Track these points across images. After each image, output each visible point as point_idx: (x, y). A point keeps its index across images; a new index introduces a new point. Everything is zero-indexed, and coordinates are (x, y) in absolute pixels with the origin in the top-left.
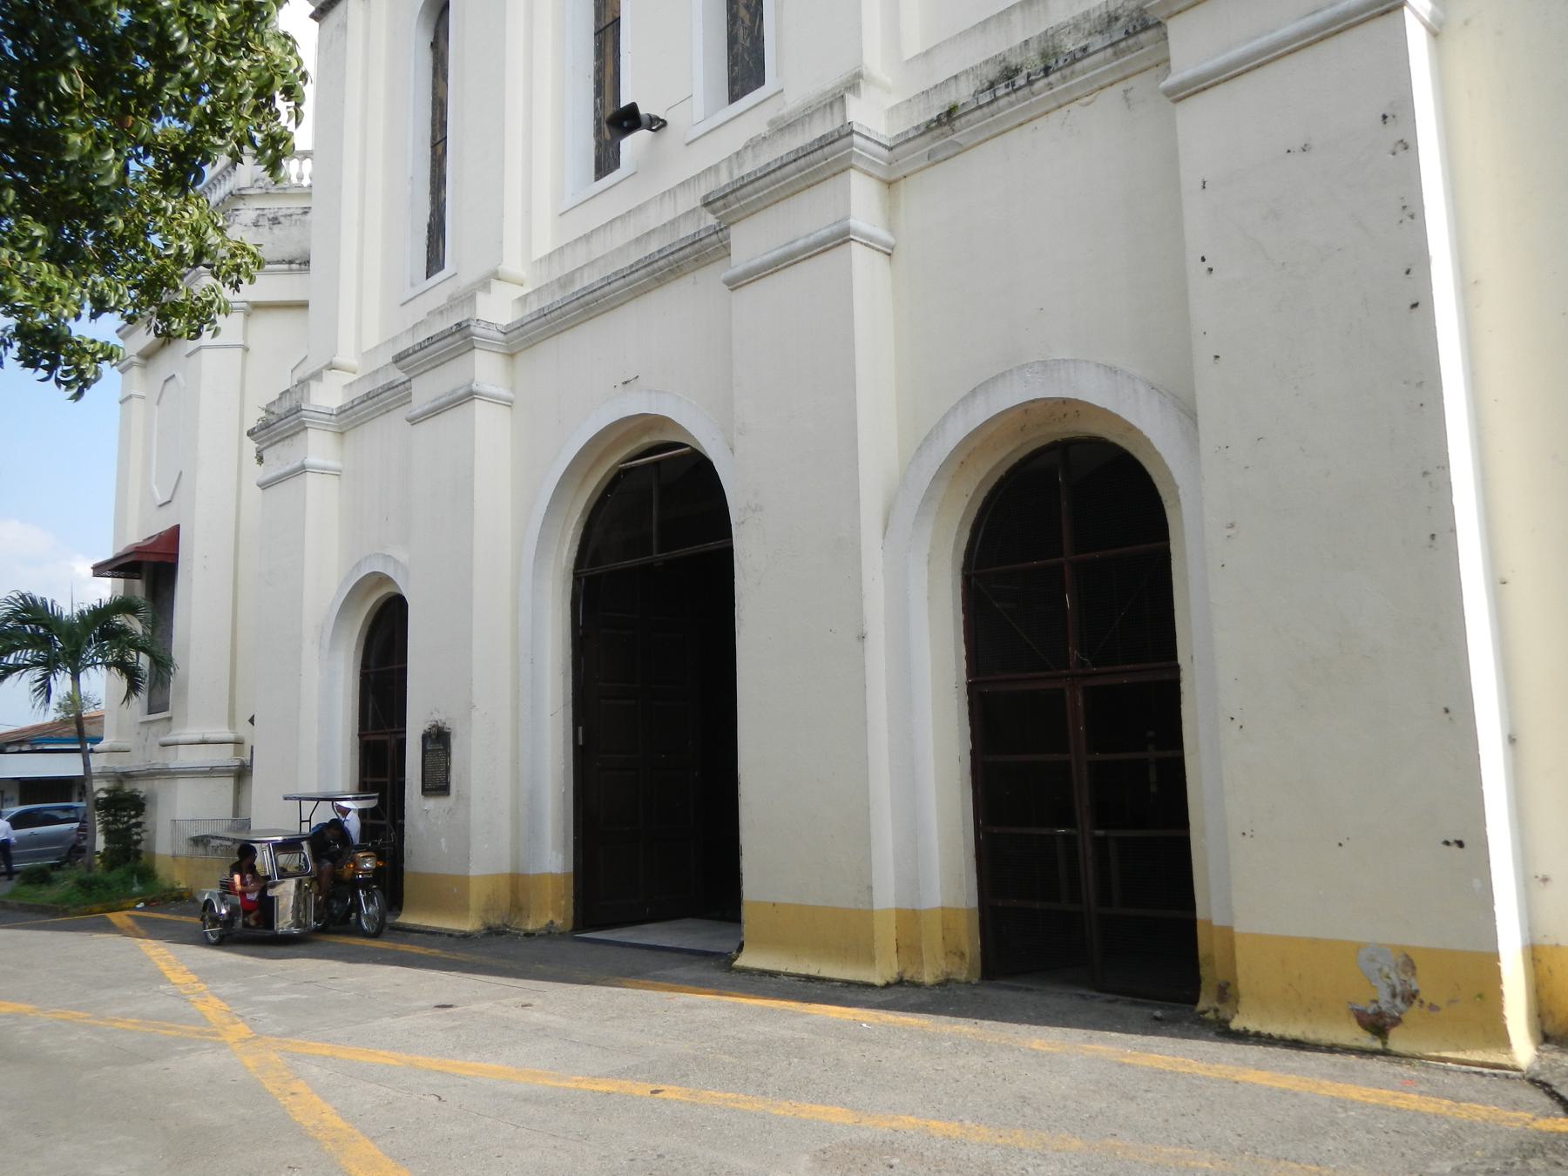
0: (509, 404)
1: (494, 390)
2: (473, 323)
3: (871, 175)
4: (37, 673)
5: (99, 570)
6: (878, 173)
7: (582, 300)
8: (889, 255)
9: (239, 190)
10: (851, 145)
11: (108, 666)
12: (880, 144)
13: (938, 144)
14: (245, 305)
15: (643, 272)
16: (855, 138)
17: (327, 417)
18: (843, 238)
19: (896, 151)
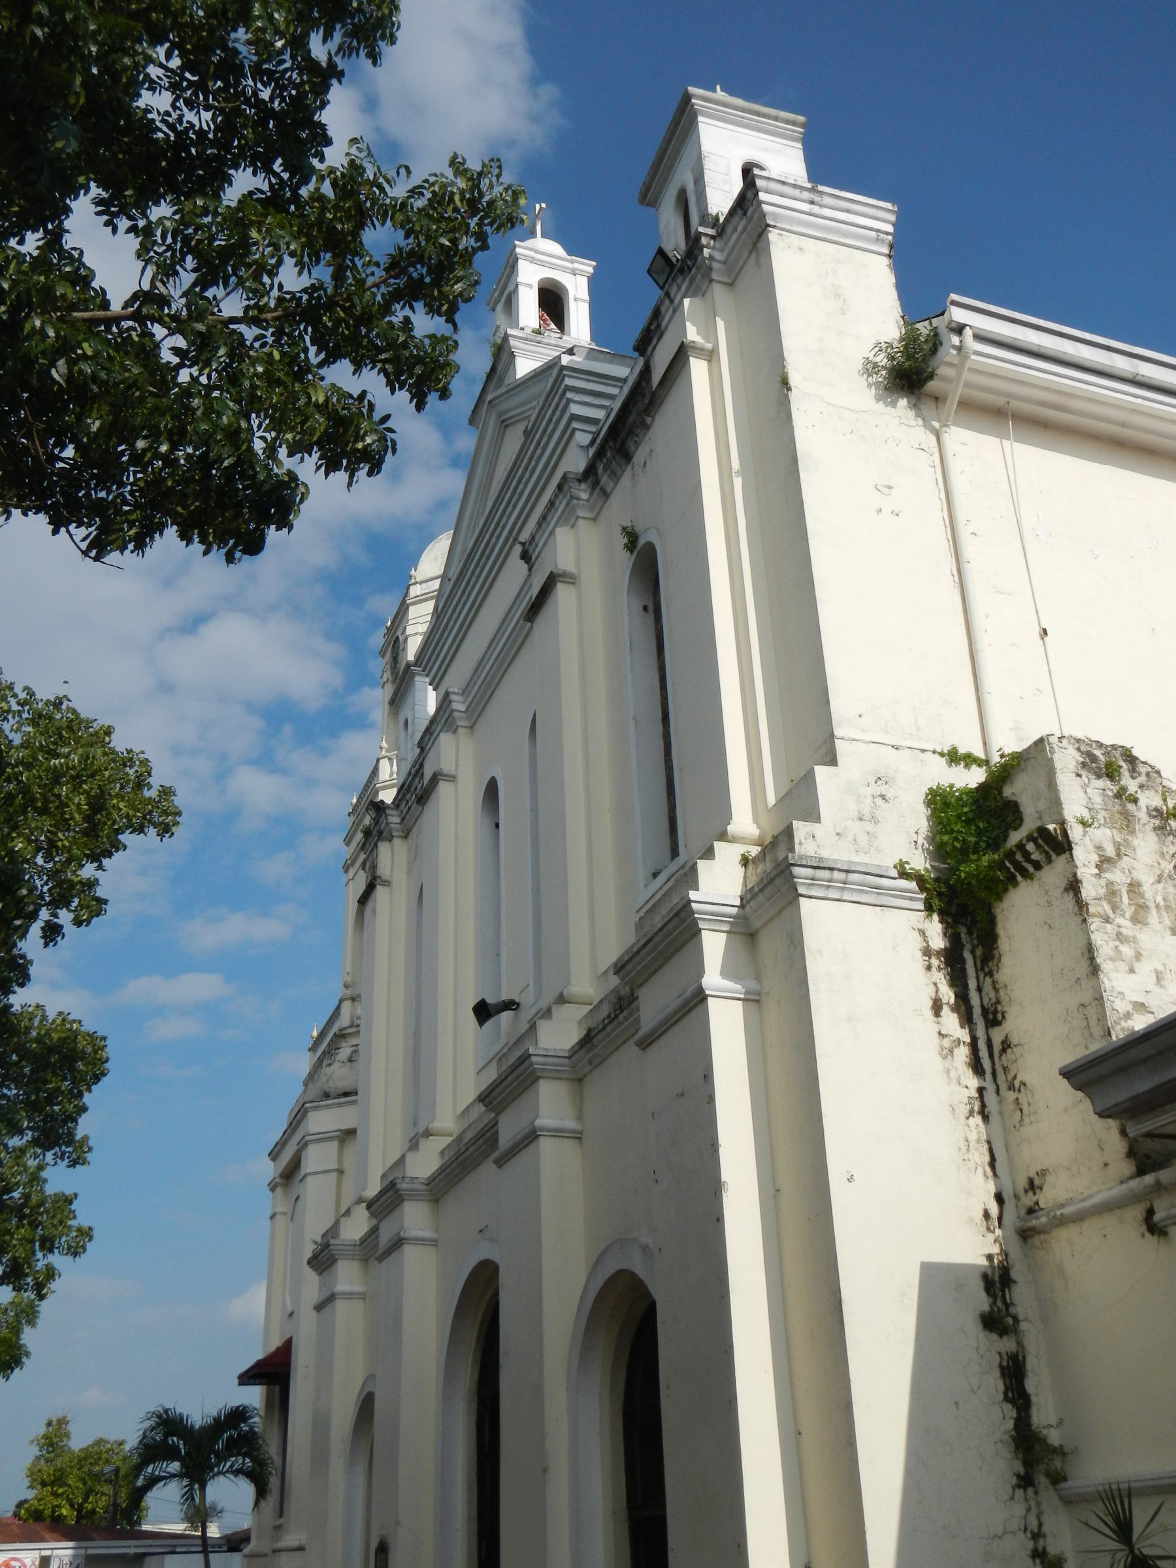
0: (434, 1243)
1: (420, 1234)
2: (398, 1181)
3: (560, 1079)
4: (185, 1482)
5: (248, 1378)
6: (565, 1076)
7: (458, 1161)
8: (580, 1138)
9: (341, 1030)
10: (532, 1064)
11: (237, 1472)
12: (559, 1057)
13: (590, 1055)
14: (338, 1133)
15: (481, 1140)
16: (534, 1059)
17: (352, 1248)
18: (532, 1136)
19: (574, 1058)
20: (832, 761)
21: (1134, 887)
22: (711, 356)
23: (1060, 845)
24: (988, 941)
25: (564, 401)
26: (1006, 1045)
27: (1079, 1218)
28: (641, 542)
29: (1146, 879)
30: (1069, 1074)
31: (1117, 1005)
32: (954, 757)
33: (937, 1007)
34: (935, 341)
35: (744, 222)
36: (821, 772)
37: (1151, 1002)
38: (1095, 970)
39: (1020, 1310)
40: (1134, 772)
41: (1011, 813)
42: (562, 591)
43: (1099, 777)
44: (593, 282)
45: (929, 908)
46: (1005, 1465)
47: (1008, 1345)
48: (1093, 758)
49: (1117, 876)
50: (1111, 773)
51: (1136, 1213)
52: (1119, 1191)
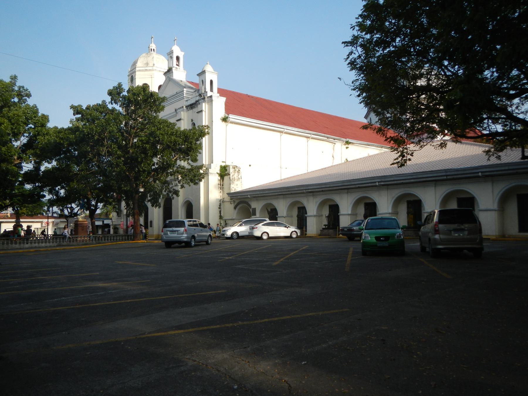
11: (114, 212)
20: (213, 163)
21: (234, 178)
22: (205, 112)
23: (230, 175)
24: (223, 179)
25: (183, 94)
26: (223, 188)
27: (226, 202)
28: (193, 122)
29: (235, 177)
30: (227, 193)
31: (231, 187)
32: (223, 162)
33: (218, 184)
34: (227, 118)
35: (210, 99)
36: (212, 164)
37: (234, 187)
38: (230, 185)
39: (221, 207)
40: (236, 168)
41: (226, 170)
42: (182, 121)
43: (233, 168)
44: (184, 56)
45: (219, 176)
46: (219, 217)
47: (220, 210)
48: (233, 167)
49: (233, 177)
50: (235, 168)
51: (230, 202)
52: (229, 200)
